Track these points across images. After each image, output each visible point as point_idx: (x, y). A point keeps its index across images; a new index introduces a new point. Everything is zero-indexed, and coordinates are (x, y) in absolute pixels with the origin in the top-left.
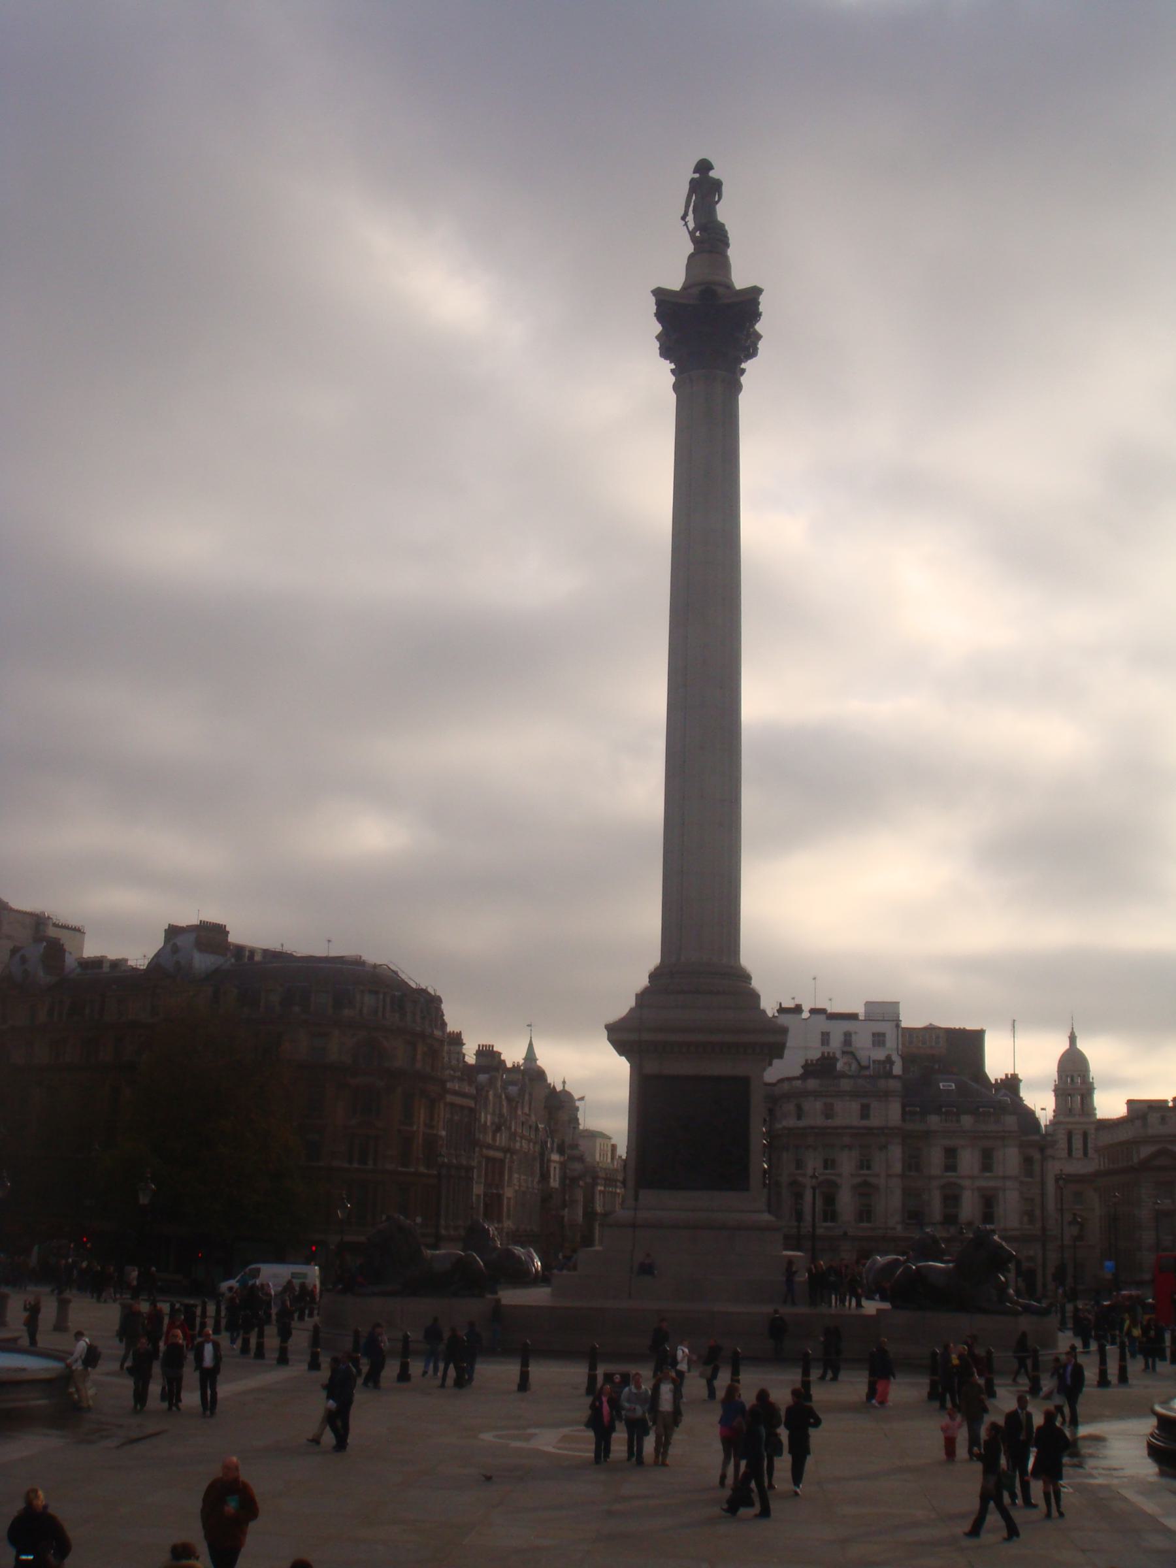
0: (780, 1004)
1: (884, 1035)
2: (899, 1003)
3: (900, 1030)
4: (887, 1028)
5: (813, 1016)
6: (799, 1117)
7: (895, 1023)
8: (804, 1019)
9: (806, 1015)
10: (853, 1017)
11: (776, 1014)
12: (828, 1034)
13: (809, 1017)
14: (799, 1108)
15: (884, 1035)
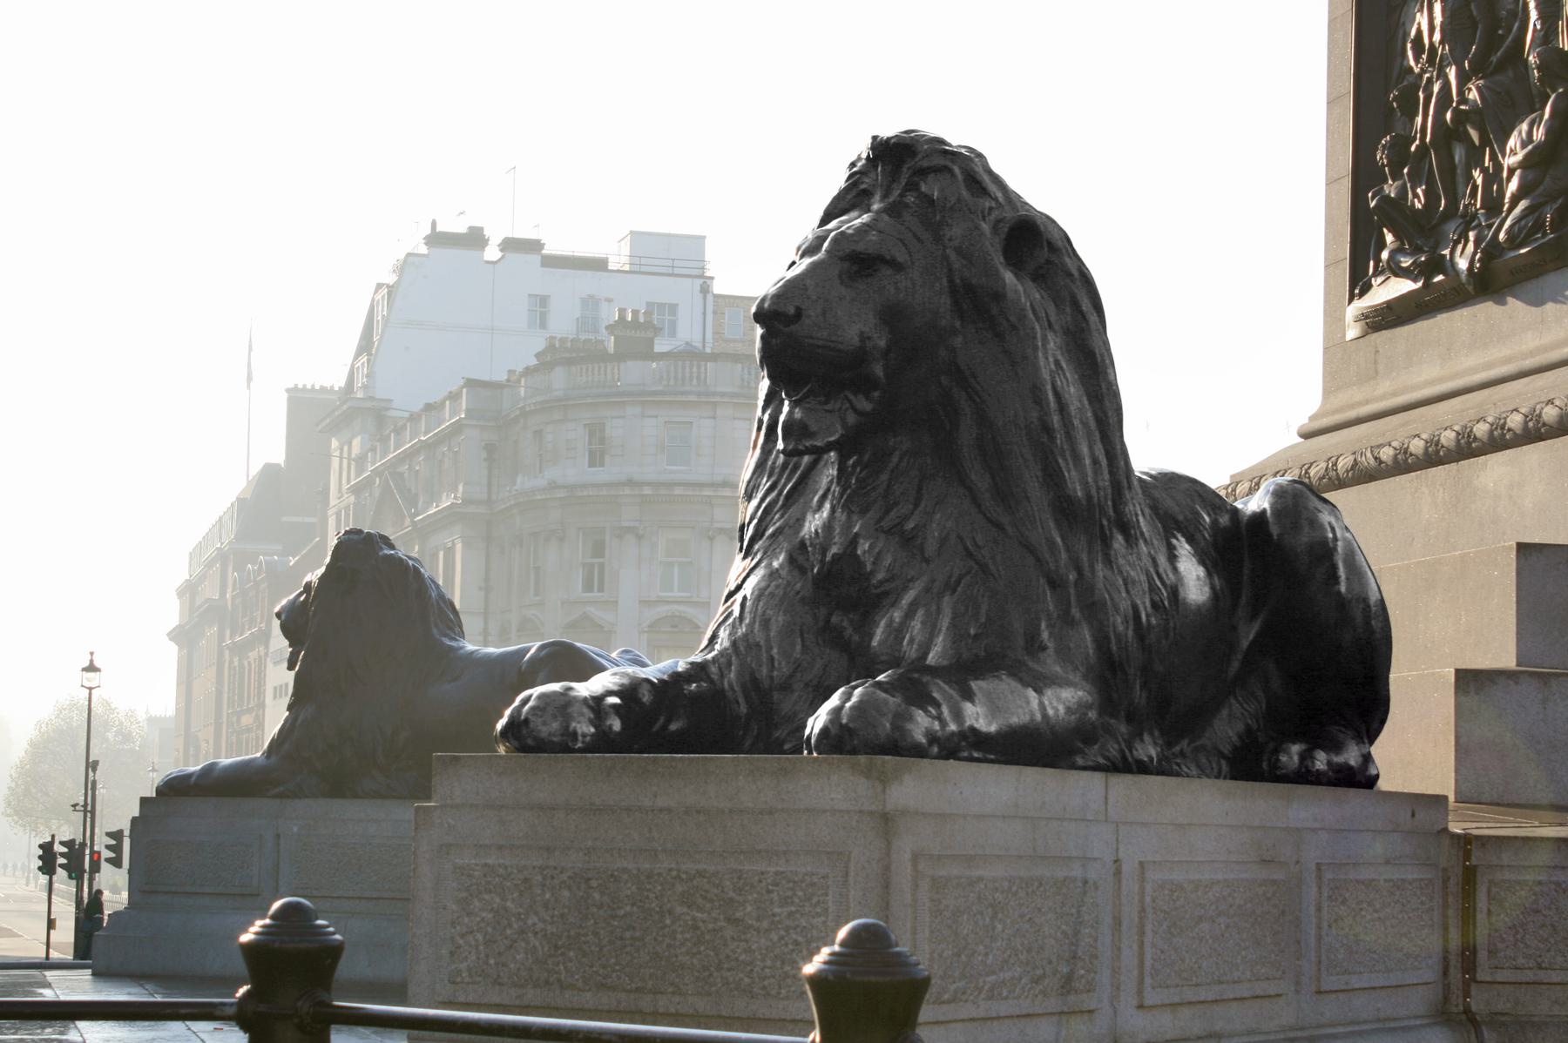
0: (434, 224)
1: (673, 308)
2: (704, 237)
3: (710, 298)
4: (680, 292)
5: (513, 257)
6: (596, 459)
7: (701, 281)
8: (488, 262)
9: (492, 253)
10: (599, 265)
11: (423, 250)
12: (543, 300)
13: (503, 257)
14: (596, 433)
15: (673, 308)
